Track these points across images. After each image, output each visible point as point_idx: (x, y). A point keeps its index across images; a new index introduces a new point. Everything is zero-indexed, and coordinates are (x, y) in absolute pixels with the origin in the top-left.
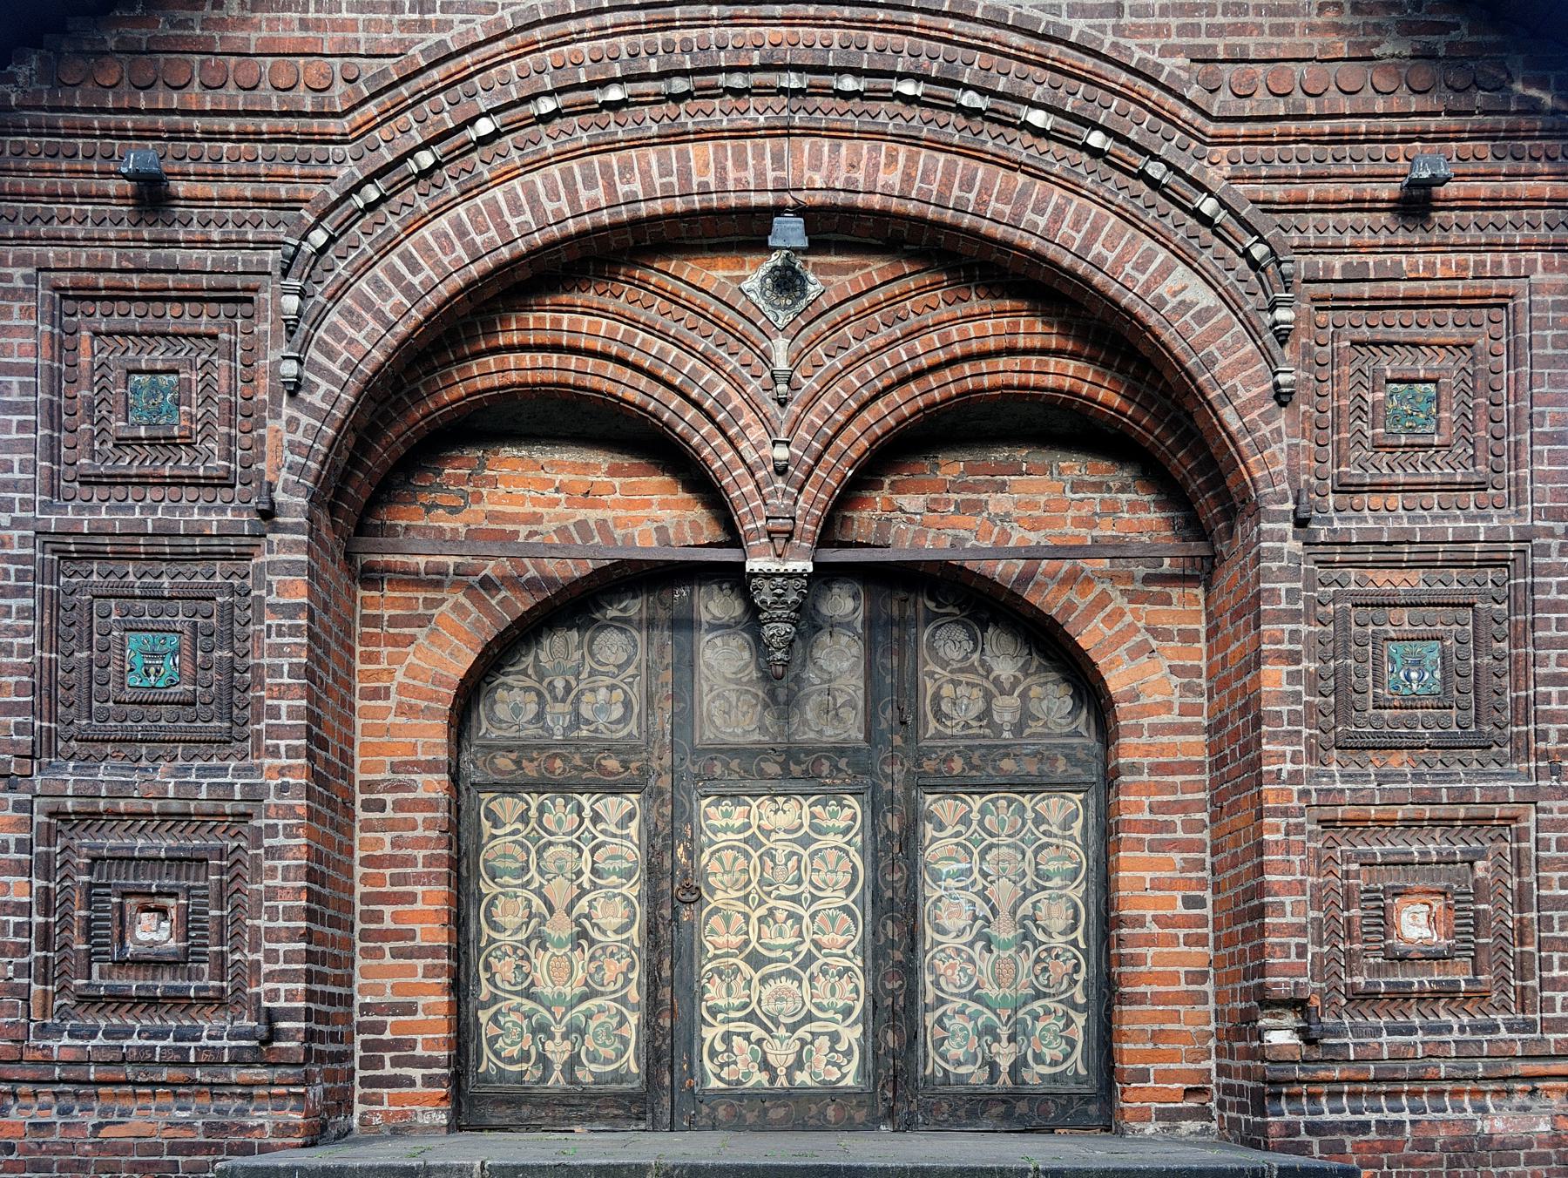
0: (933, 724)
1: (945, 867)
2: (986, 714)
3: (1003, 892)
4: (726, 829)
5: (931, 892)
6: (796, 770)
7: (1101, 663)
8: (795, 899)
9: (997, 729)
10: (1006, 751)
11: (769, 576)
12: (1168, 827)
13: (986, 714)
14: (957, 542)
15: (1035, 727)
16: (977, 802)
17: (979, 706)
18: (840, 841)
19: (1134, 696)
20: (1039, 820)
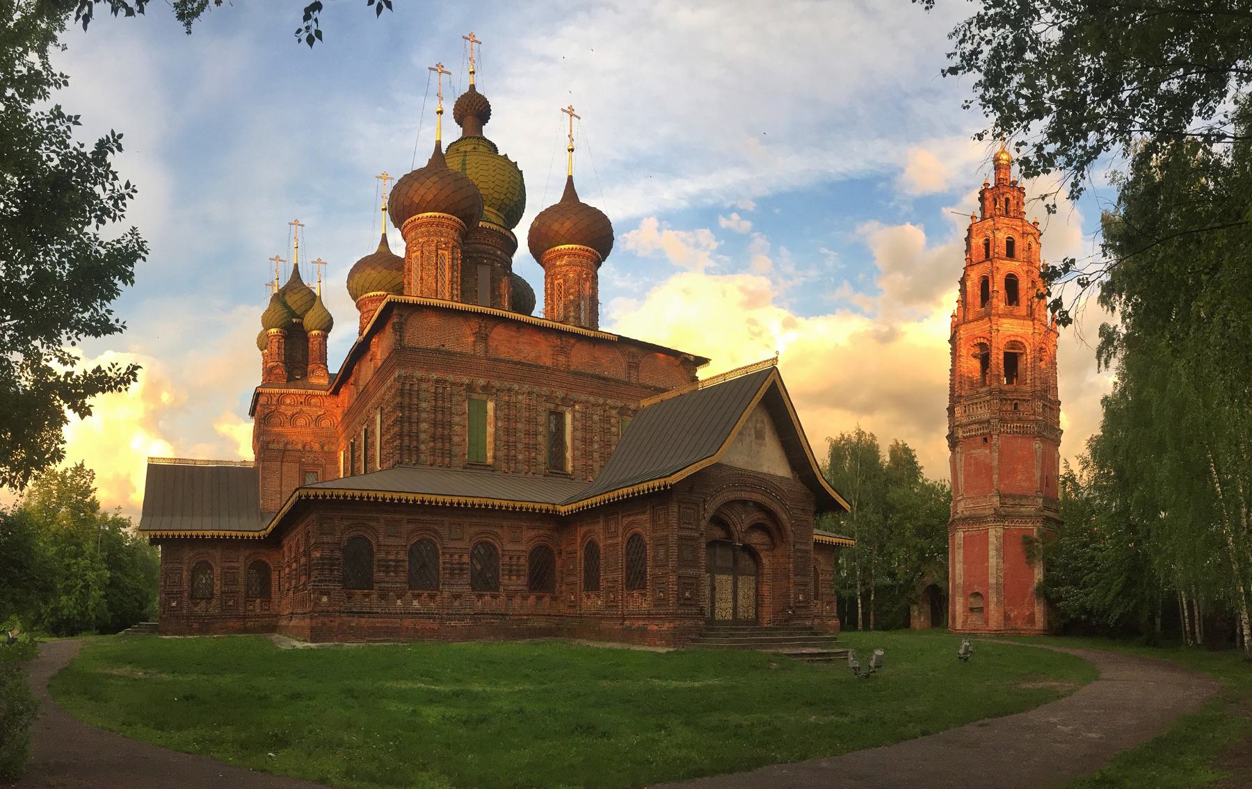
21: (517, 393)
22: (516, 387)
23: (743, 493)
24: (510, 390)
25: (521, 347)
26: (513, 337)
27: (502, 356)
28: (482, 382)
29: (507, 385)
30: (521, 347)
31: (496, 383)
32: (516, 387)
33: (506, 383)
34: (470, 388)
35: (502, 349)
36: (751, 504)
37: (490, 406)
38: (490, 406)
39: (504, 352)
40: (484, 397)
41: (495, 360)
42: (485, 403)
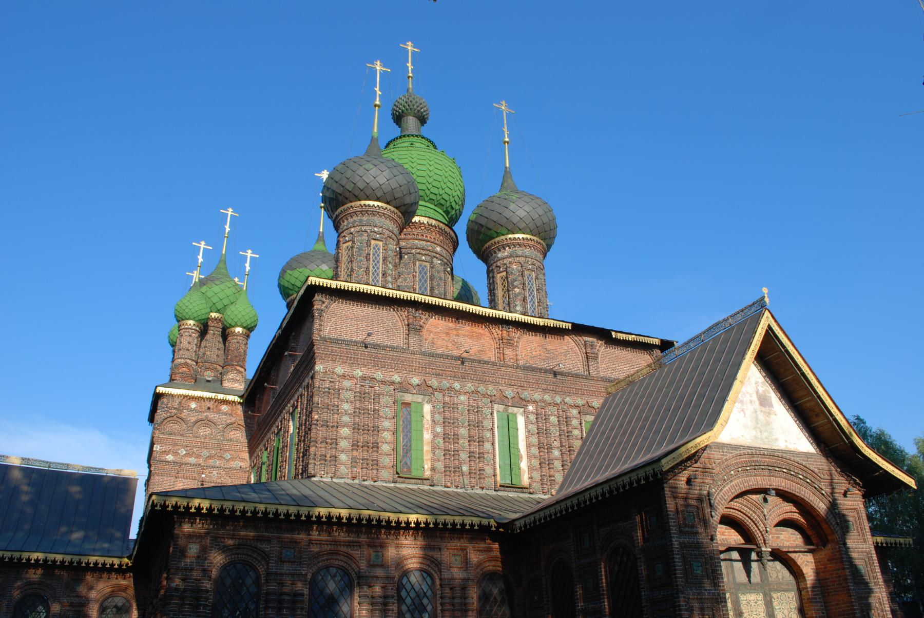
0: (770, 579)
1: (777, 607)
2: (777, 577)
3: (786, 612)
4: (744, 600)
5: (776, 613)
6: (752, 588)
7: (801, 567)
8: (756, 615)
9: (779, 579)
10: (781, 583)
11: (765, 551)
12: (816, 599)
13: (777, 577)
14: (778, 544)
15: (785, 579)
16: (779, 594)
17: (776, 575)
18: (761, 602)
19: (807, 574)
20: (789, 598)
21: (458, 393)
22: (457, 386)
23: (759, 478)
24: (450, 389)
25: (461, 340)
26: (450, 329)
27: (440, 351)
28: (415, 380)
29: (446, 384)
30: (461, 340)
31: (434, 382)
32: (457, 386)
33: (445, 382)
34: (403, 387)
35: (440, 342)
36: (773, 492)
37: (427, 408)
38: (427, 408)
39: (442, 346)
40: (419, 398)
41: (432, 355)
42: (421, 405)
